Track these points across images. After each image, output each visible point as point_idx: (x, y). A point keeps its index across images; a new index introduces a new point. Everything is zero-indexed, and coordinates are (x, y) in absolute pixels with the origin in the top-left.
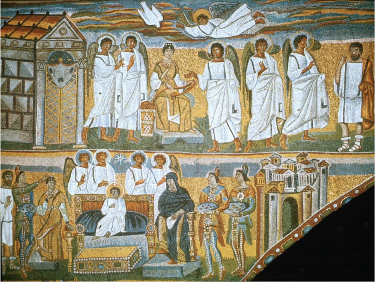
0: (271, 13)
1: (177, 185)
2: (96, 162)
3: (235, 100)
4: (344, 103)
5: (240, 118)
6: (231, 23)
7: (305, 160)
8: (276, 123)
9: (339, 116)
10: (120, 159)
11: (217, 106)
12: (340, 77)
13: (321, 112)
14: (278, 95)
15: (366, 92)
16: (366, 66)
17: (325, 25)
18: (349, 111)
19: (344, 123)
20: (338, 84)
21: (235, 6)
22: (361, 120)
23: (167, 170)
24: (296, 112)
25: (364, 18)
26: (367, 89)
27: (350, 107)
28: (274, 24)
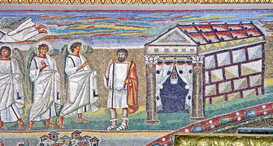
0: (52, 26)
3: (19, 89)
4: (113, 93)
5: (23, 103)
6: (19, 32)
7: (79, 136)
8: (54, 108)
9: (108, 103)
11: (3, 94)
12: (109, 74)
13: (93, 100)
14: (57, 86)
15: (131, 85)
16: (131, 66)
17: (96, 36)
18: (117, 99)
19: (112, 108)
20: (108, 79)
21: (22, 20)
22: (127, 106)
24: (72, 99)
25: (129, 32)
26: (131, 83)
27: (118, 97)
28: (53, 34)
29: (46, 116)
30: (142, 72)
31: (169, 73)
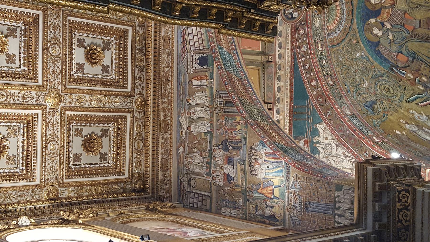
1: (221, 145)
2: (214, 174)
10: (213, 165)
20: (197, 88)
23: (217, 148)
24: (203, 102)
29: (209, 112)
30: (196, 74)
31: (196, 64)
